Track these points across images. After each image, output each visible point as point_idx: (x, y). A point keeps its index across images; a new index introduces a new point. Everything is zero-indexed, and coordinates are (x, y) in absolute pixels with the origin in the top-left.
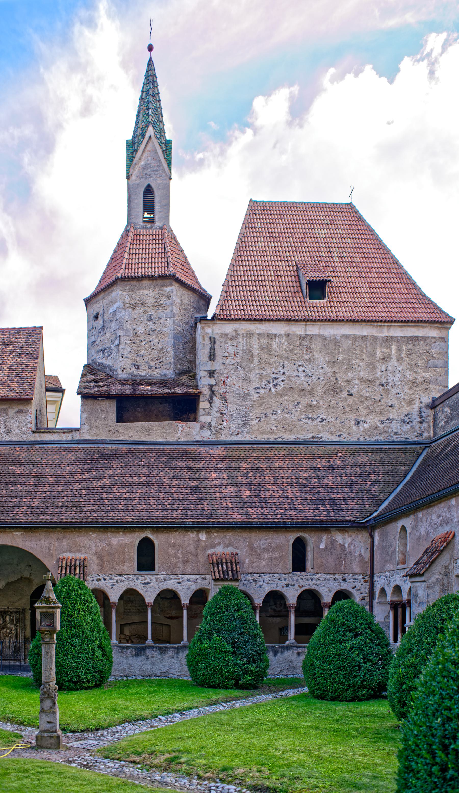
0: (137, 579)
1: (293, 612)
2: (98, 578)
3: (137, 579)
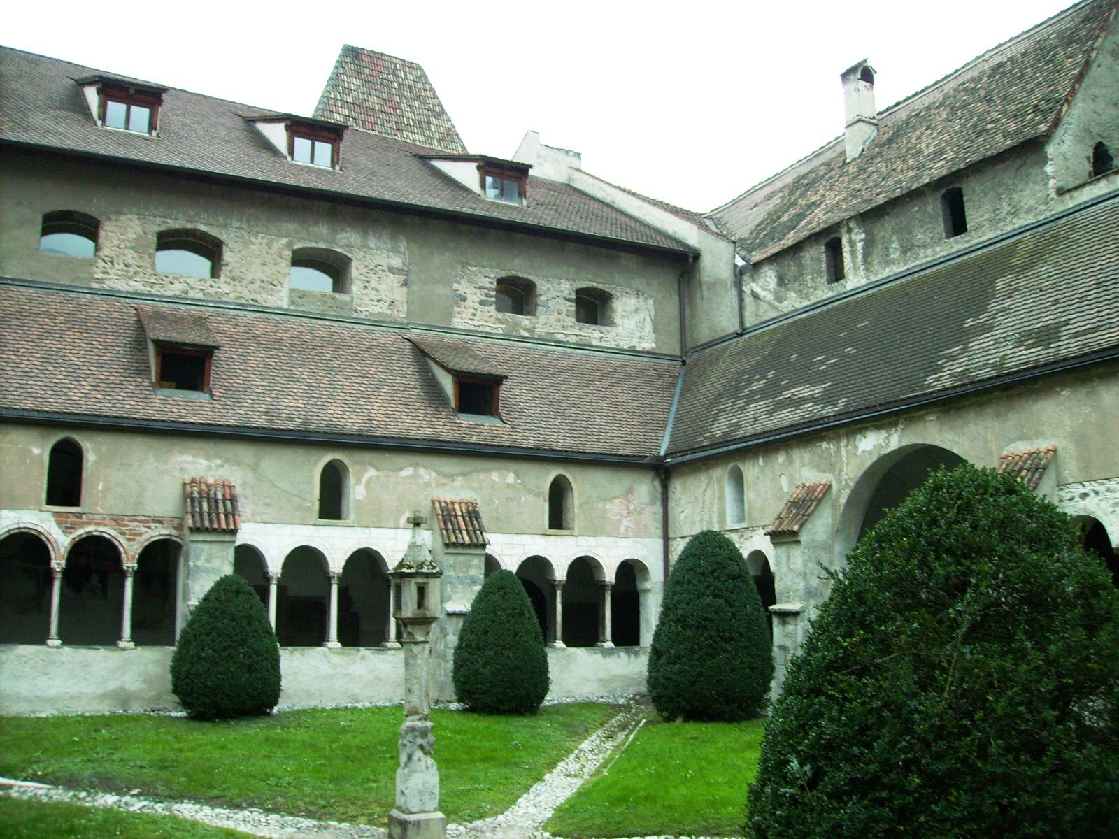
1: (609, 593)
2: (1083, 490)
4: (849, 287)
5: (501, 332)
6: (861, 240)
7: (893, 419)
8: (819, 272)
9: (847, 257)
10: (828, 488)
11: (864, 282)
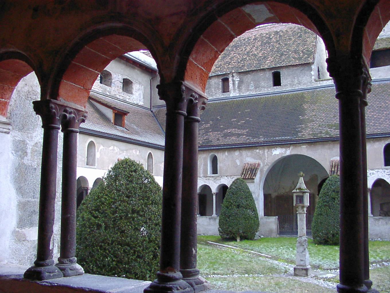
0: (384, 172)
3: (384, 172)
4: (231, 96)
5: (101, 92)
6: (237, 81)
7: (289, 145)
8: (218, 88)
9: (231, 85)
10: (259, 165)
11: (238, 95)
